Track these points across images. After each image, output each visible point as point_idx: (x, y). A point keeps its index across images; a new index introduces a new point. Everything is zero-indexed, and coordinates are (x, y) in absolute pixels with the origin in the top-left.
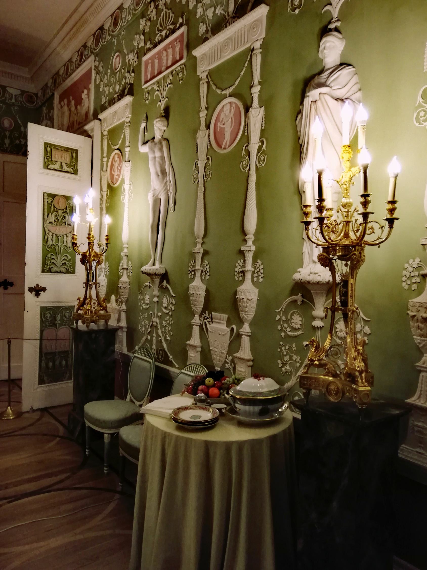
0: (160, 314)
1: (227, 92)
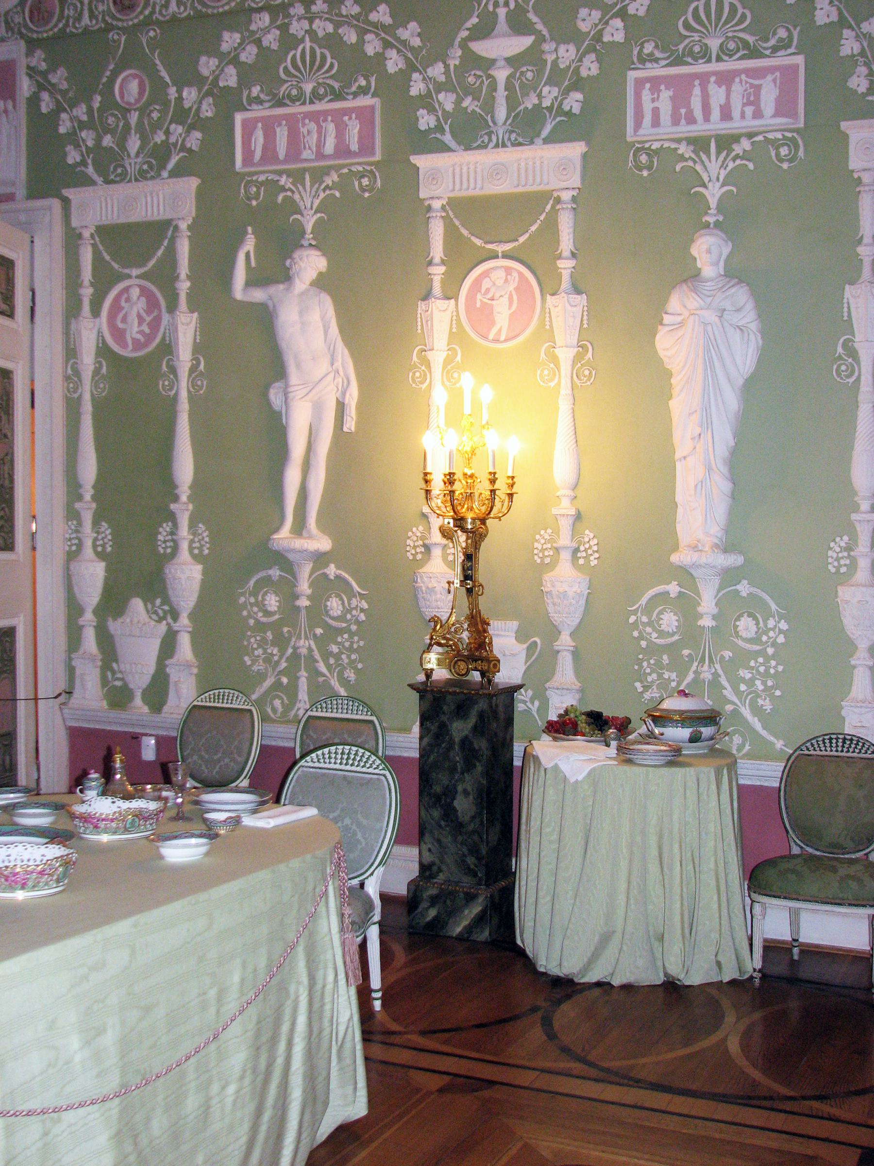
1: (501, 248)
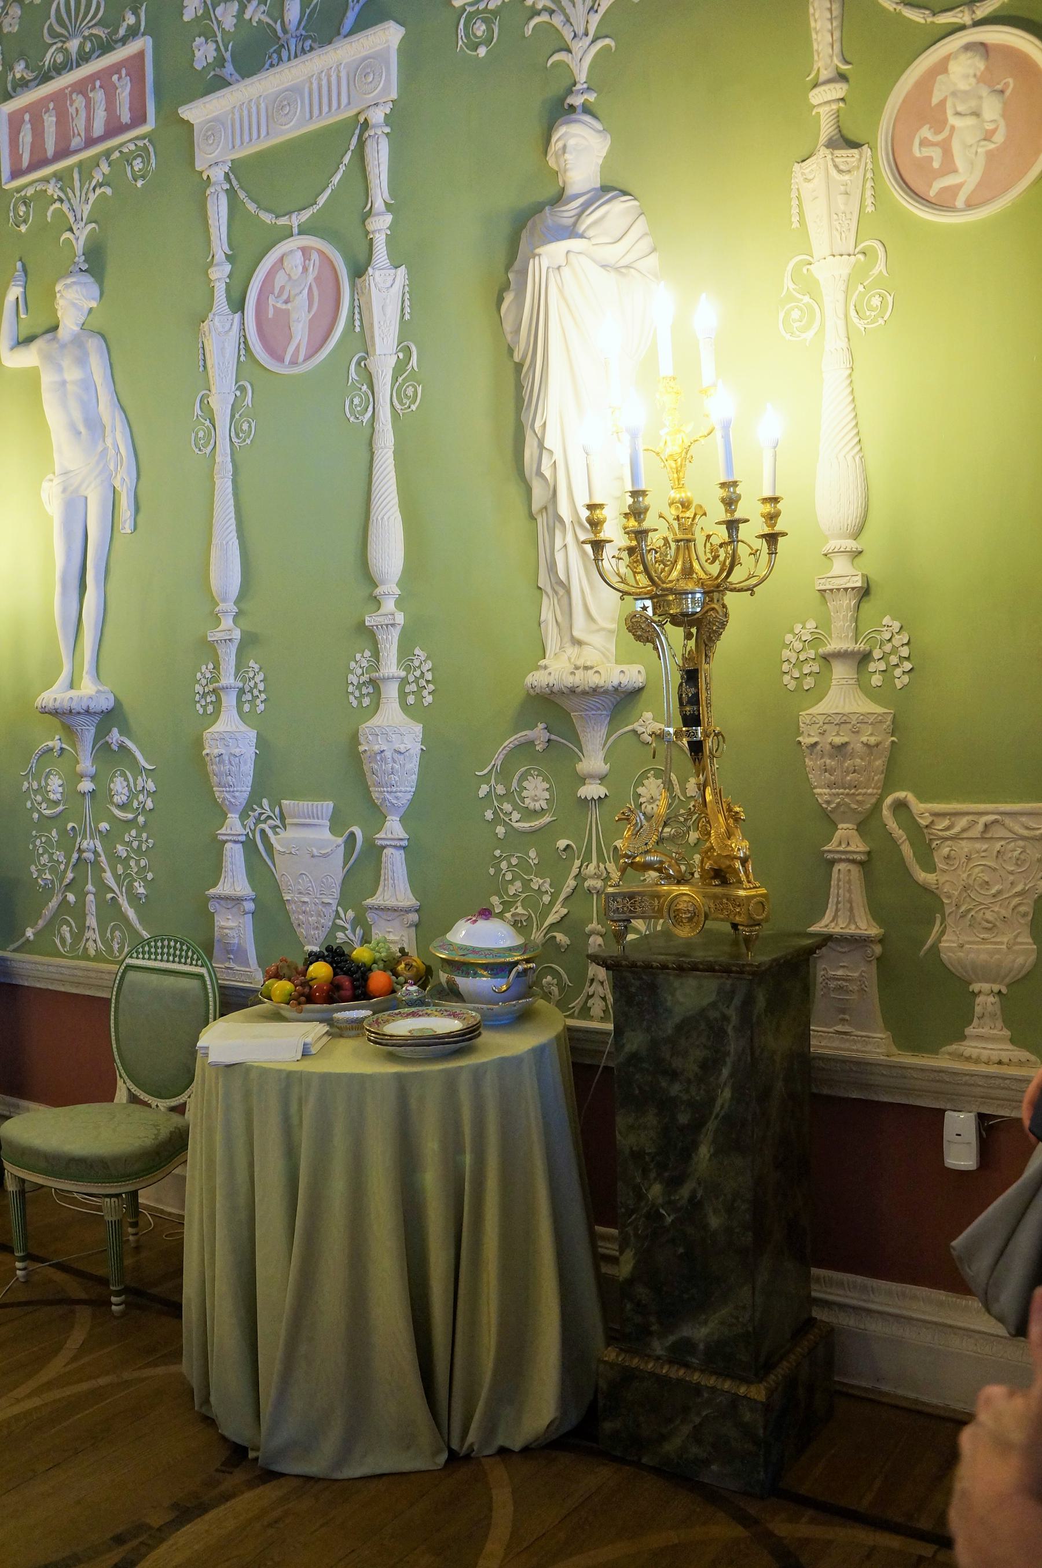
0: (104, 826)
1: (295, 221)
